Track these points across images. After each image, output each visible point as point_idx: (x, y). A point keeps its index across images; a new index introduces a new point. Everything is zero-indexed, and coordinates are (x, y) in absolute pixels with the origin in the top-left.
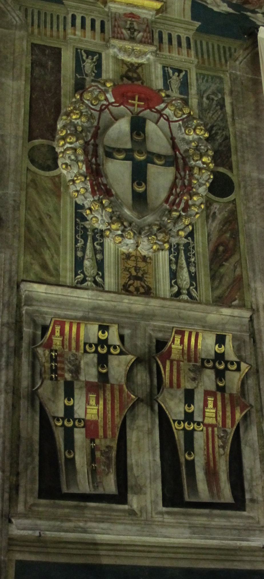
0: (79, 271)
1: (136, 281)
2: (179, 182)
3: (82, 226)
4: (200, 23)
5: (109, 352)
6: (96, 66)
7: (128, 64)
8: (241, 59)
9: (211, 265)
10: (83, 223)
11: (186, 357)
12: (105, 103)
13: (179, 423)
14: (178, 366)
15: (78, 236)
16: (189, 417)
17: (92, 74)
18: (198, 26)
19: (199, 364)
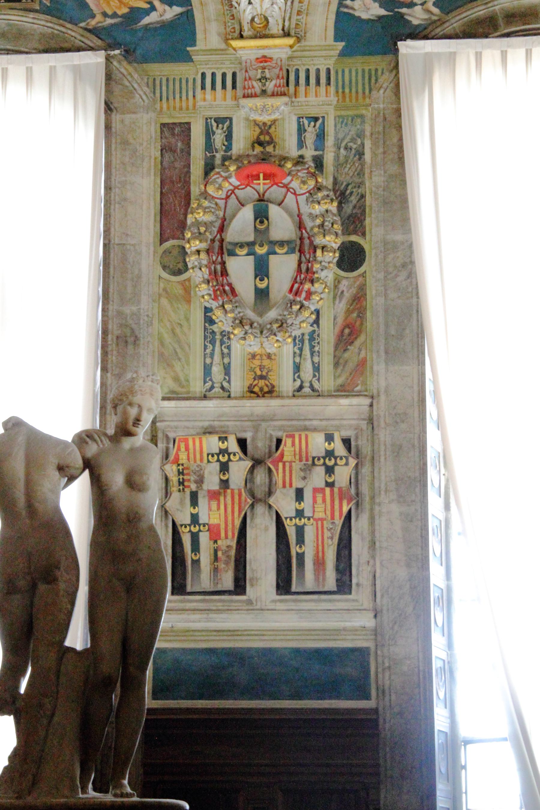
0: (208, 379)
1: (260, 381)
2: (304, 267)
3: (211, 331)
4: (343, 44)
5: (229, 460)
6: (226, 136)
7: (261, 124)
8: (385, 86)
9: (335, 351)
10: (211, 327)
11: (297, 457)
12: (232, 188)
13: (291, 520)
14: (291, 467)
15: (207, 342)
16: (300, 514)
17: (222, 148)
18: (340, 48)
19: (310, 462)
